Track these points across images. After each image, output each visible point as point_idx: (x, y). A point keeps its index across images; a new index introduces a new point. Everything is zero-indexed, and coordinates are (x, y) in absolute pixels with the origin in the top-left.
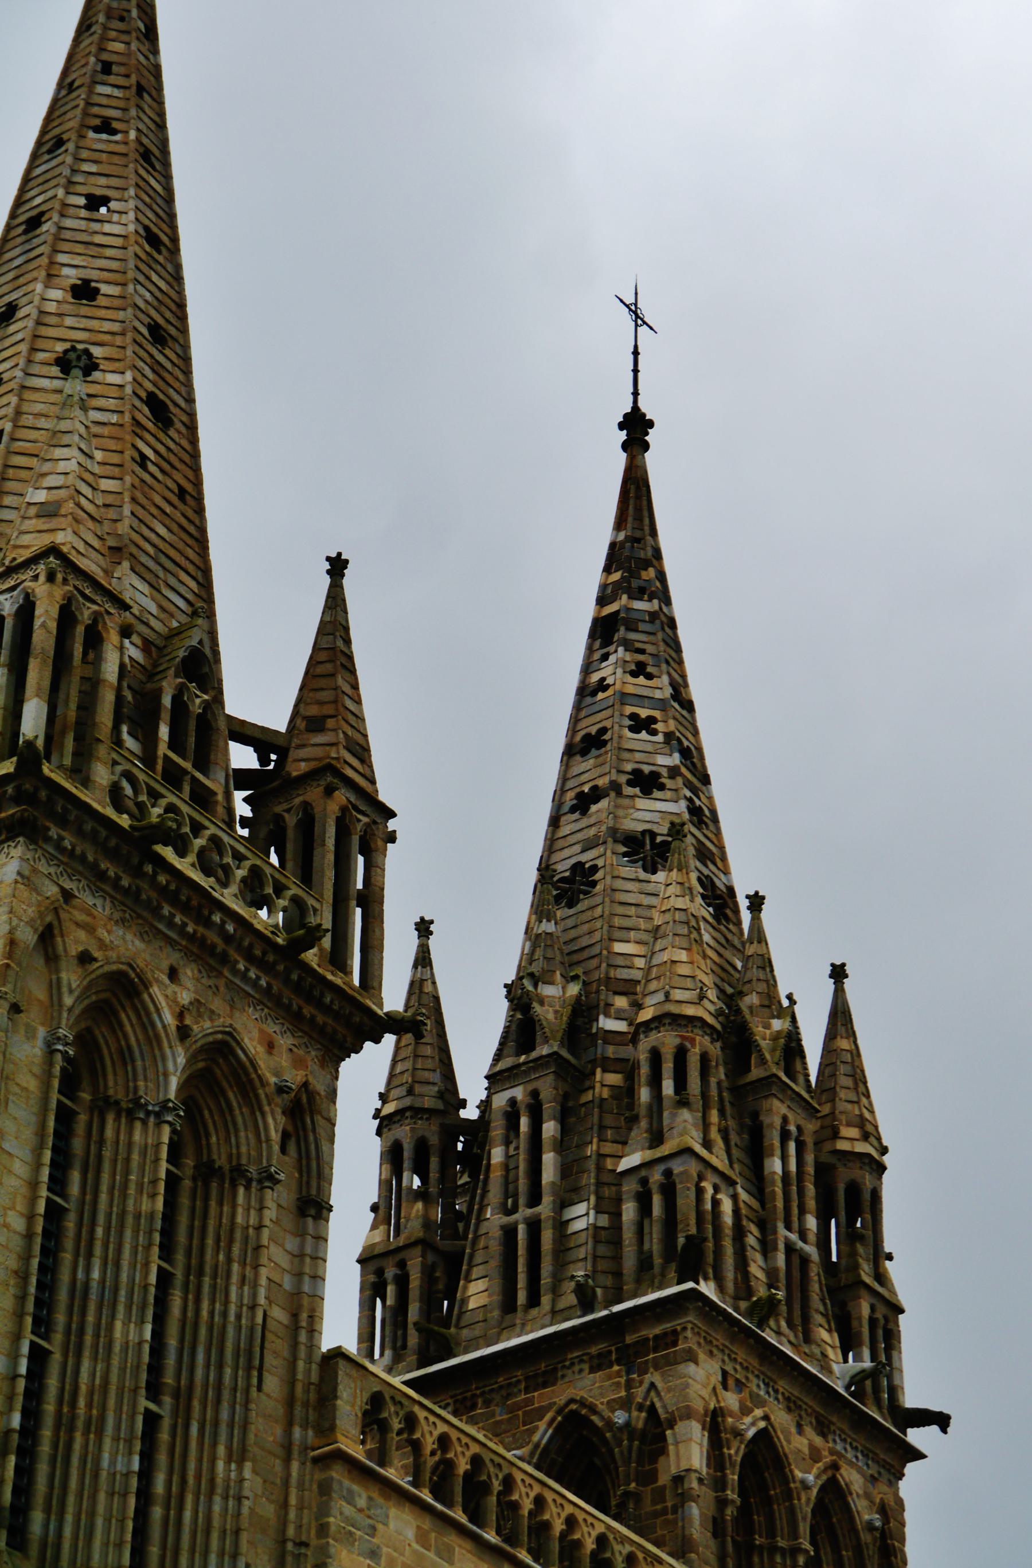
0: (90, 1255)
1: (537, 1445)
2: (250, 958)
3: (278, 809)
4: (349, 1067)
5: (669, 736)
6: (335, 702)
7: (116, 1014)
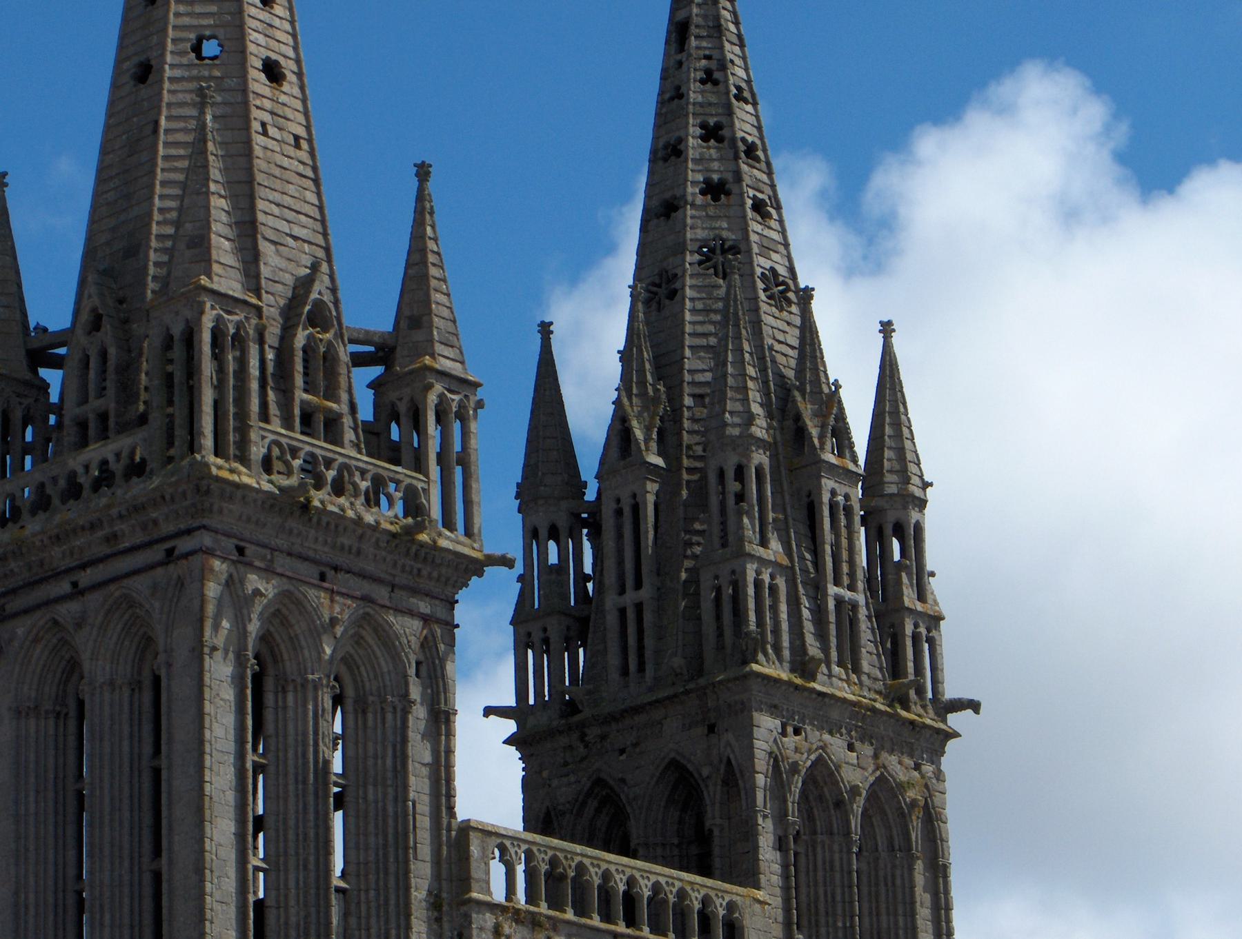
3: (392, 396)
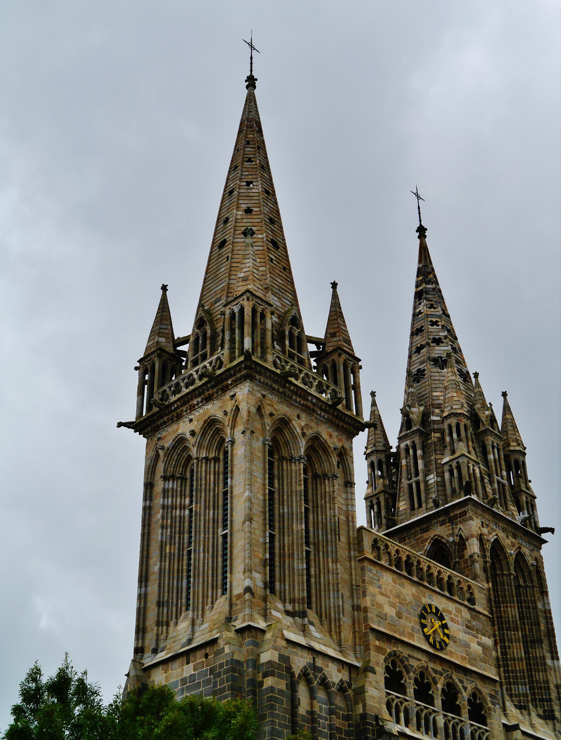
0: (283, 505)
1: (426, 550)
2: (321, 409)
3: (325, 362)
4: (356, 440)
5: (443, 326)
6: (338, 327)
7: (282, 431)
